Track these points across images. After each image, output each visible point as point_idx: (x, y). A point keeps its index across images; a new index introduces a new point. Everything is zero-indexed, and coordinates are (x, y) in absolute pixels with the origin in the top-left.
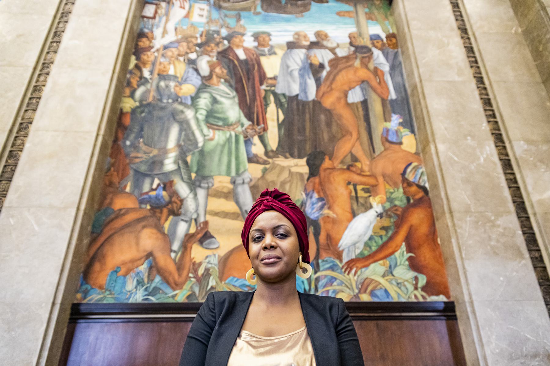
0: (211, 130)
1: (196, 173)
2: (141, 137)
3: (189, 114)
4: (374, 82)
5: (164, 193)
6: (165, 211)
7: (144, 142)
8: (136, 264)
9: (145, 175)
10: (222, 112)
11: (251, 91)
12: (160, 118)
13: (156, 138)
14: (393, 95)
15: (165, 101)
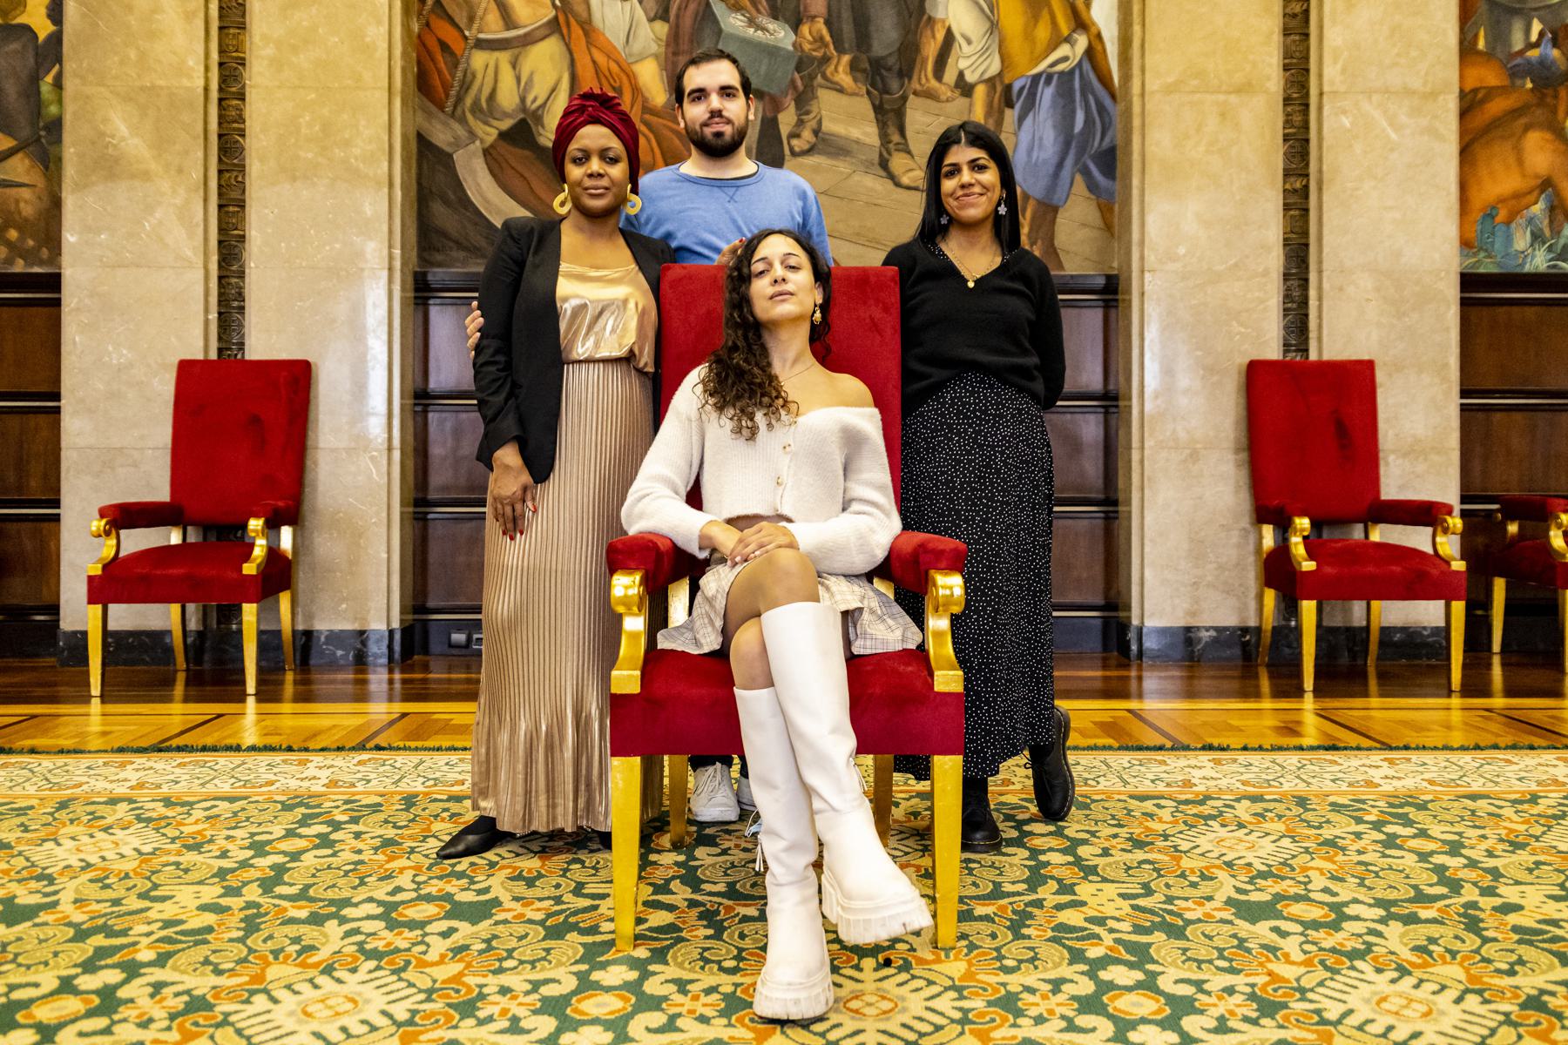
5: (1555, 53)
8: (1525, 201)
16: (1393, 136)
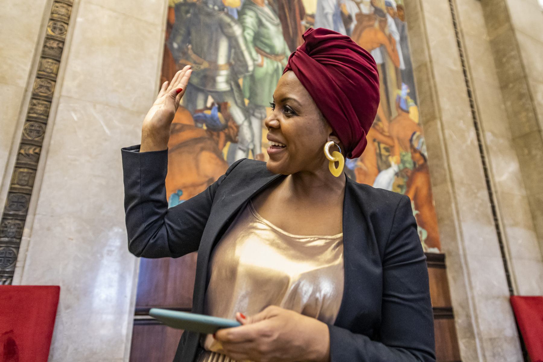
0: (259, 56)
1: (249, 99)
2: (190, 42)
3: (237, 30)
4: (390, 49)
5: (219, 115)
6: (222, 135)
7: (192, 49)
9: (198, 90)
10: (268, 38)
11: (293, 23)
12: (208, 26)
13: (205, 48)
14: (402, 66)
15: (211, 6)
16: (107, 131)
